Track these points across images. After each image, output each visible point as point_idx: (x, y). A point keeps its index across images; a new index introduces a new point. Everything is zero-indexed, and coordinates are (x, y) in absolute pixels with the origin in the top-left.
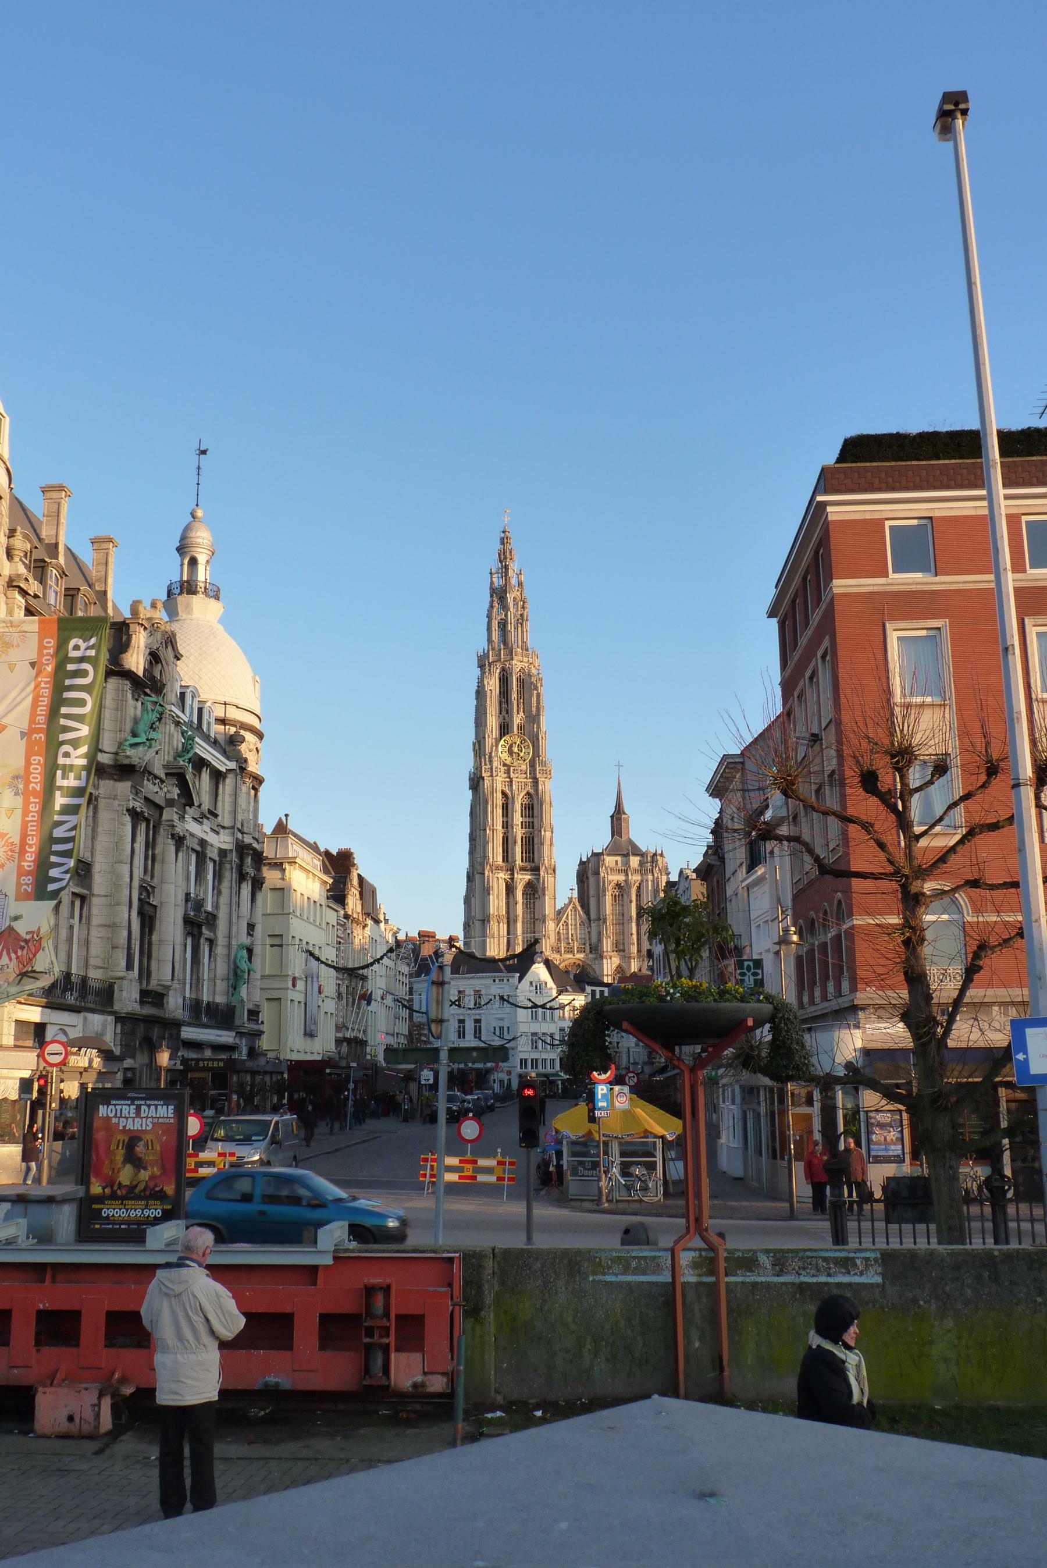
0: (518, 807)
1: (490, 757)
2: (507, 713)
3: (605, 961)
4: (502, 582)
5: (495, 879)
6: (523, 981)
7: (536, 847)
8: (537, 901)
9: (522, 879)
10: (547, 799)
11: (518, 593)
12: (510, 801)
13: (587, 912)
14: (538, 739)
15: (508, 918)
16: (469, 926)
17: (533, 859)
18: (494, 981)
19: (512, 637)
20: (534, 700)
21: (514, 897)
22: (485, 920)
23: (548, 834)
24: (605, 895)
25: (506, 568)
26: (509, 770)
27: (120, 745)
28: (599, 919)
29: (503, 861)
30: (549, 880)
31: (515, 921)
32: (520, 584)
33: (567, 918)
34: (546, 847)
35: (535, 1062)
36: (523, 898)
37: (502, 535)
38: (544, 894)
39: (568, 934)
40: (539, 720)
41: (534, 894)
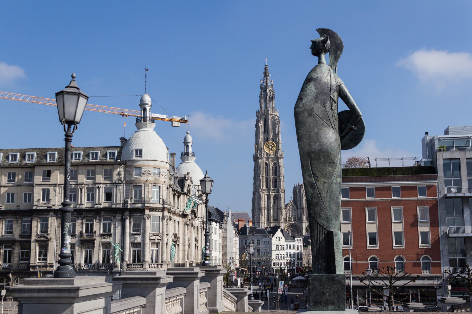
0: (271, 168)
1: (261, 150)
2: (267, 134)
3: (303, 224)
4: (265, 84)
5: (263, 195)
6: (274, 237)
7: (278, 182)
8: (278, 202)
9: (272, 194)
10: (282, 165)
11: (271, 89)
12: (268, 166)
13: (297, 207)
14: (278, 143)
15: (268, 208)
16: (254, 211)
17: (277, 186)
18: (264, 237)
19: (269, 105)
20: (277, 128)
21: (270, 201)
22: (260, 209)
23: (282, 178)
24: (303, 200)
25: (267, 79)
26: (268, 155)
27: (184, 210)
28: (301, 208)
29: (266, 188)
30: (283, 195)
31: (271, 209)
32: (272, 85)
33: (289, 208)
34: (281, 183)
35: (278, 264)
36: (273, 201)
37: (265, 67)
38: (281, 200)
39: (289, 214)
40: (279, 136)
41: (277, 200)
